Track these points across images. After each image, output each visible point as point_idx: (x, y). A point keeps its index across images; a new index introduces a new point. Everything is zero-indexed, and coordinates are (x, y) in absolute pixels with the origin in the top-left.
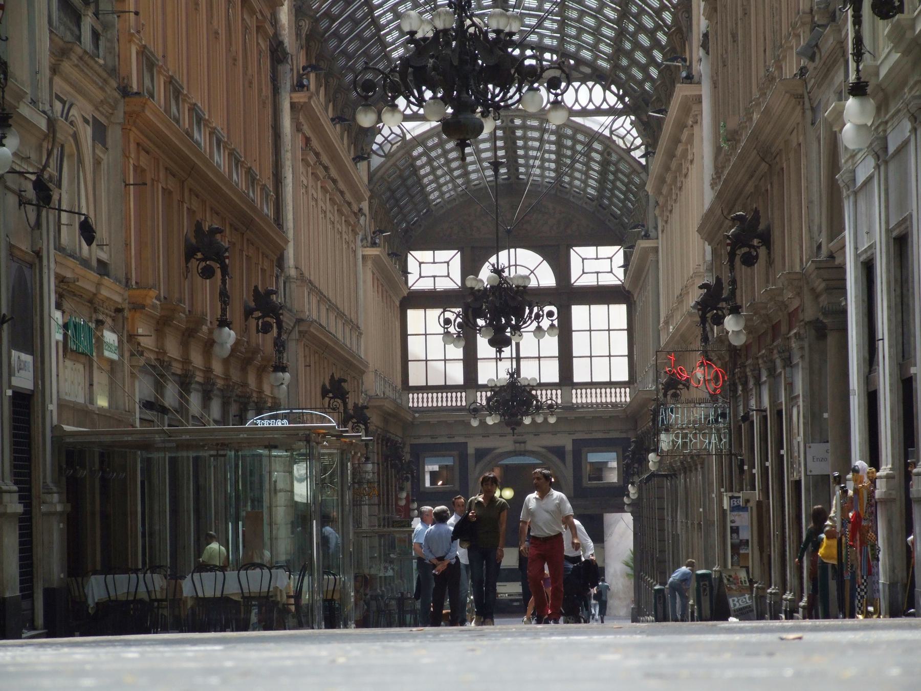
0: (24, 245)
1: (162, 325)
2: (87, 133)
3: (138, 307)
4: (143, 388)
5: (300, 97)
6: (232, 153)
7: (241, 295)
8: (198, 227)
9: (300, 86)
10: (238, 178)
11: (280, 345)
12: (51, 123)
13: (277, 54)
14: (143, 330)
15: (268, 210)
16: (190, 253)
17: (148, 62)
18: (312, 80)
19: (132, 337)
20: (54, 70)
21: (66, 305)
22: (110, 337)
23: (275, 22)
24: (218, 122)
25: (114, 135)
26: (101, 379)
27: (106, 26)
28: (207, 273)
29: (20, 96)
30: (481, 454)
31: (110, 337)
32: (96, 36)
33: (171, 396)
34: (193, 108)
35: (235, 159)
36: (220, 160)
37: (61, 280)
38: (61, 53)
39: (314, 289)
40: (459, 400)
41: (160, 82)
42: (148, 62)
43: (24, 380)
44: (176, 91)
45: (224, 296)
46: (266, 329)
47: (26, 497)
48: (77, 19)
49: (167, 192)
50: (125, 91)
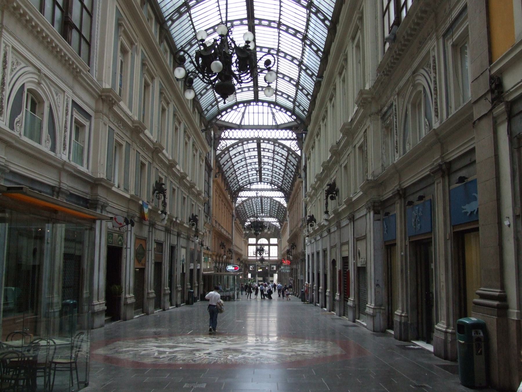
0: (199, 250)
1: (216, 256)
2: (208, 232)
3: (213, 254)
4: (214, 265)
5: (235, 221)
6: (226, 231)
7: (227, 249)
8: (222, 242)
9: (235, 220)
10: (227, 235)
11: (232, 256)
12: (203, 234)
13: (233, 216)
14: (214, 258)
15: (231, 237)
16: (220, 246)
17: (216, 222)
18: (237, 219)
19: (213, 258)
20: (204, 225)
21: (205, 256)
22: (210, 259)
23: (233, 212)
24: (225, 228)
25: (211, 232)
26: (208, 264)
27: (211, 218)
28: (223, 248)
29: (200, 231)
30: (258, 266)
31: (210, 259)
32: (209, 219)
33: (217, 265)
34: (222, 227)
35: (227, 232)
36: (225, 233)
37: (204, 253)
38: (205, 223)
39: (236, 246)
40: (255, 258)
41: (218, 224)
42: (216, 222)
43: (199, 267)
44: (219, 225)
45: (225, 251)
46: (230, 254)
47: (198, 283)
48: (207, 218)
49: (218, 238)
50: (213, 226)
